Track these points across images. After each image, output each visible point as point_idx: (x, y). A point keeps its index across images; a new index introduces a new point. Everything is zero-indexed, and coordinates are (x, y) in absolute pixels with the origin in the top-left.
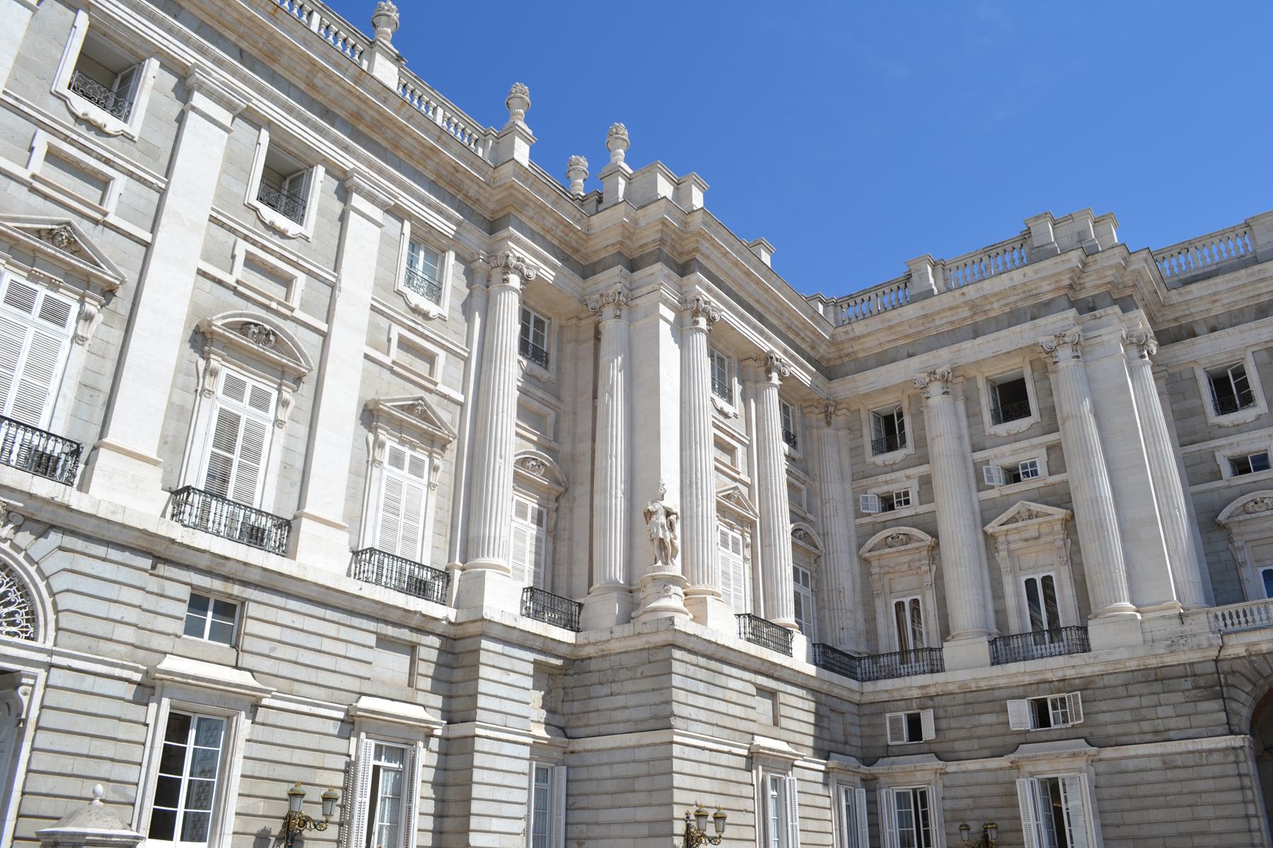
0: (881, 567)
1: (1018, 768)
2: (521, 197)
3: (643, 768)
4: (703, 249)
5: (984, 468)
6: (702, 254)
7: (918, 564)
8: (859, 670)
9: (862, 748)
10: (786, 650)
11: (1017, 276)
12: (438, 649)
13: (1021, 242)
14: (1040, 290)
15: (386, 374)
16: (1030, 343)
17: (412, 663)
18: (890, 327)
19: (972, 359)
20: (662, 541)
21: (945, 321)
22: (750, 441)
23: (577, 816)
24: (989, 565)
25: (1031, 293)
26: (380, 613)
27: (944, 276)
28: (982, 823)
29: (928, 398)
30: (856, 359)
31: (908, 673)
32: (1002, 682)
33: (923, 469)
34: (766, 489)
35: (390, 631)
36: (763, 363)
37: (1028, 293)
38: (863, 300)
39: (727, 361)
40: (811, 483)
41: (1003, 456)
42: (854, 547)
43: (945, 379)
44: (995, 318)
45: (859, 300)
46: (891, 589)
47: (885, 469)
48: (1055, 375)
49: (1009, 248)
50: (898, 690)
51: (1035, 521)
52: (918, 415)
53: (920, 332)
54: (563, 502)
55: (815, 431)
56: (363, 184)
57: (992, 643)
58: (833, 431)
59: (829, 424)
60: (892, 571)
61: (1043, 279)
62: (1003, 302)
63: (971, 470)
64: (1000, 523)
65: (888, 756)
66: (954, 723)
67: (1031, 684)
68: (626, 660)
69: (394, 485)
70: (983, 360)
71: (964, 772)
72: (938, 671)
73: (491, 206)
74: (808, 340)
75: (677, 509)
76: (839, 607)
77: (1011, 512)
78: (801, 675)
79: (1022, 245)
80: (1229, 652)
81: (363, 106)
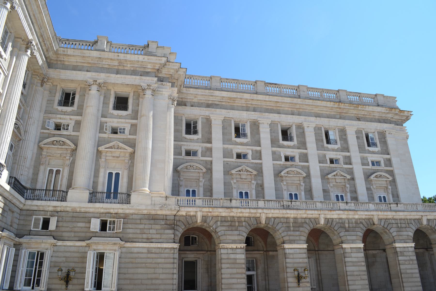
0: (47, 153)
1: (89, 247)
5: (105, 124)
7: (65, 155)
8: (26, 194)
9: (17, 230)
11: (141, 58)
13: (143, 48)
14: (147, 67)
16: (137, 84)
18: (84, 57)
19: (113, 82)
21: (107, 63)
22: (8, 74)
24: (96, 163)
25: (143, 66)
27: (110, 48)
28: (67, 269)
29: (90, 90)
31: (50, 199)
32: (91, 210)
33: (78, 118)
34: (9, 99)
36: (26, 43)
37: (142, 66)
38: (73, 44)
39: (9, 34)
40: (26, 107)
41: (113, 122)
42: (37, 141)
43: (99, 85)
44: (127, 70)
45: (71, 43)
46: (49, 163)
47: (61, 113)
48: (142, 99)
49: (138, 49)
50: (43, 206)
51: (119, 150)
52: (83, 96)
53: (95, 64)
55: (35, 86)
57: (90, 193)
58: (42, 90)
59: (42, 86)
60: (52, 155)
61: (150, 63)
62: (132, 65)
63: (99, 124)
64: (105, 147)
65: (30, 235)
66: (65, 224)
67: (103, 213)
70: (117, 83)
71: (65, 246)
72: (63, 201)
74: (47, 46)
76: (23, 165)
77: (111, 144)
78: (2, 188)
79: (143, 50)
80: (180, 213)
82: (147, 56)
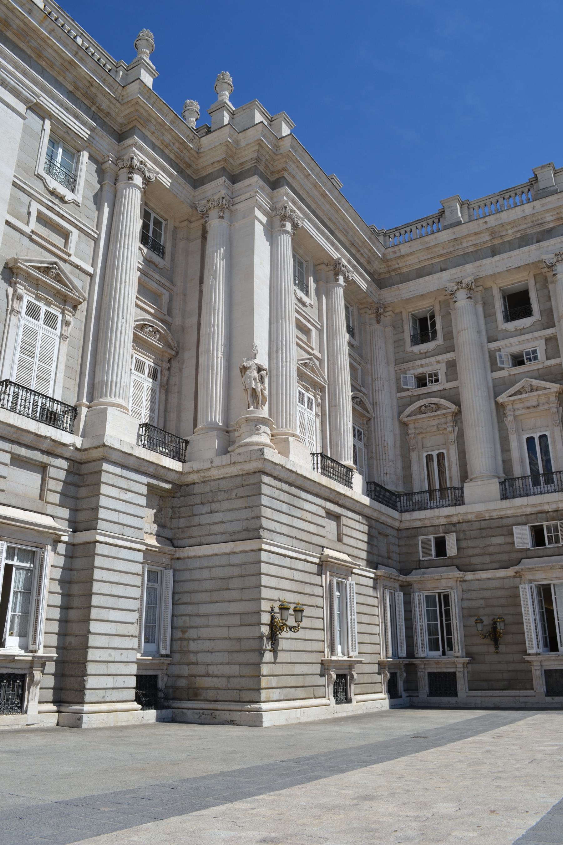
0: (416, 429)
1: (520, 577)
2: (145, 114)
3: (236, 571)
4: (291, 170)
5: (497, 354)
6: (290, 174)
7: (444, 426)
8: (399, 504)
9: (400, 562)
10: (348, 483)
11: (528, 209)
12: (66, 470)
13: (528, 187)
14: (545, 220)
15: (26, 241)
16: (535, 260)
17: (43, 480)
18: (428, 248)
19: (490, 272)
20: (254, 390)
21: (470, 243)
22: (321, 326)
23: (182, 609)
24: (499, 427)
25: (538, 222)
26: (15, 436)
27: (469, 213)
28: (492, 618)
29: (455, 302)
30: (401, 273)
31: (437, 506)
32: (509, 512)
33: (449, 356)
34: (334, 363)
35: (23, 452)
36: (332, 268)
37: (535, 223)
38: (406, 232)
39: (305, 264)
40: (365, 365)
41: (511, 345)
42: (396, 414)
43: (469, 288)
44: (509, 241)
45: (403, 232)
46: (423, 445)
47: (421, 356)
48: (553, 285)
49: (519, 192)
50: (429, 519)
51: (535, 393)
52: (447, 315)
53: (450, 253)
54: (174, 363)
55: (368, 327)
56: (9, 79)
57: (501, 483)
58: (381, 327)
59: (378, 322)
60: (424, 431)
61: (547, 211)
62: (516, 229)
64: (508, 395)
65: (420, 568)
66: (471, 544)
67: (531, 514)
68: (224, 484)
69: (30, 333)
70: (498, 273)
71: (478, 580)
72: (460, 505)
73: (120, 120)
74: (366, 256)
75: (266, 365)
76: (384, 458)
78: (359, 504)
79: (529, 190)
81: (10, 15)
82: (538, 201)
